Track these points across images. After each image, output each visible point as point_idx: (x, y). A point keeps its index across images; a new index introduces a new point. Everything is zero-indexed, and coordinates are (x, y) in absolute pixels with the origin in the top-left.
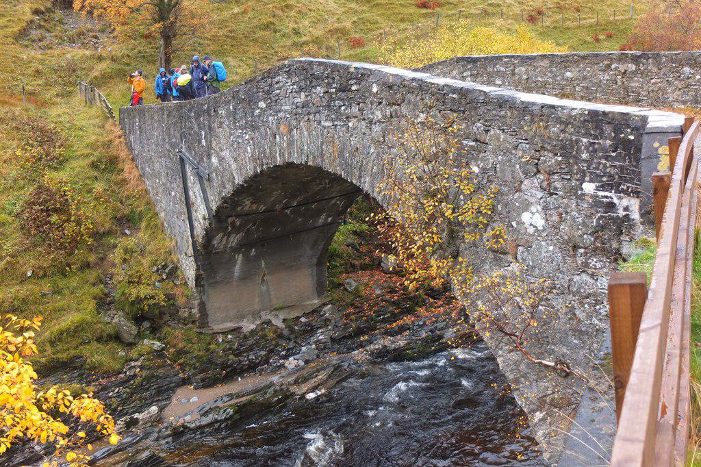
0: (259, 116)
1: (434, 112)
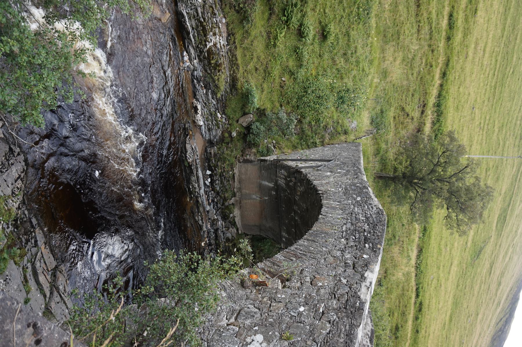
0: (352, 197)
1: (347, 289)
